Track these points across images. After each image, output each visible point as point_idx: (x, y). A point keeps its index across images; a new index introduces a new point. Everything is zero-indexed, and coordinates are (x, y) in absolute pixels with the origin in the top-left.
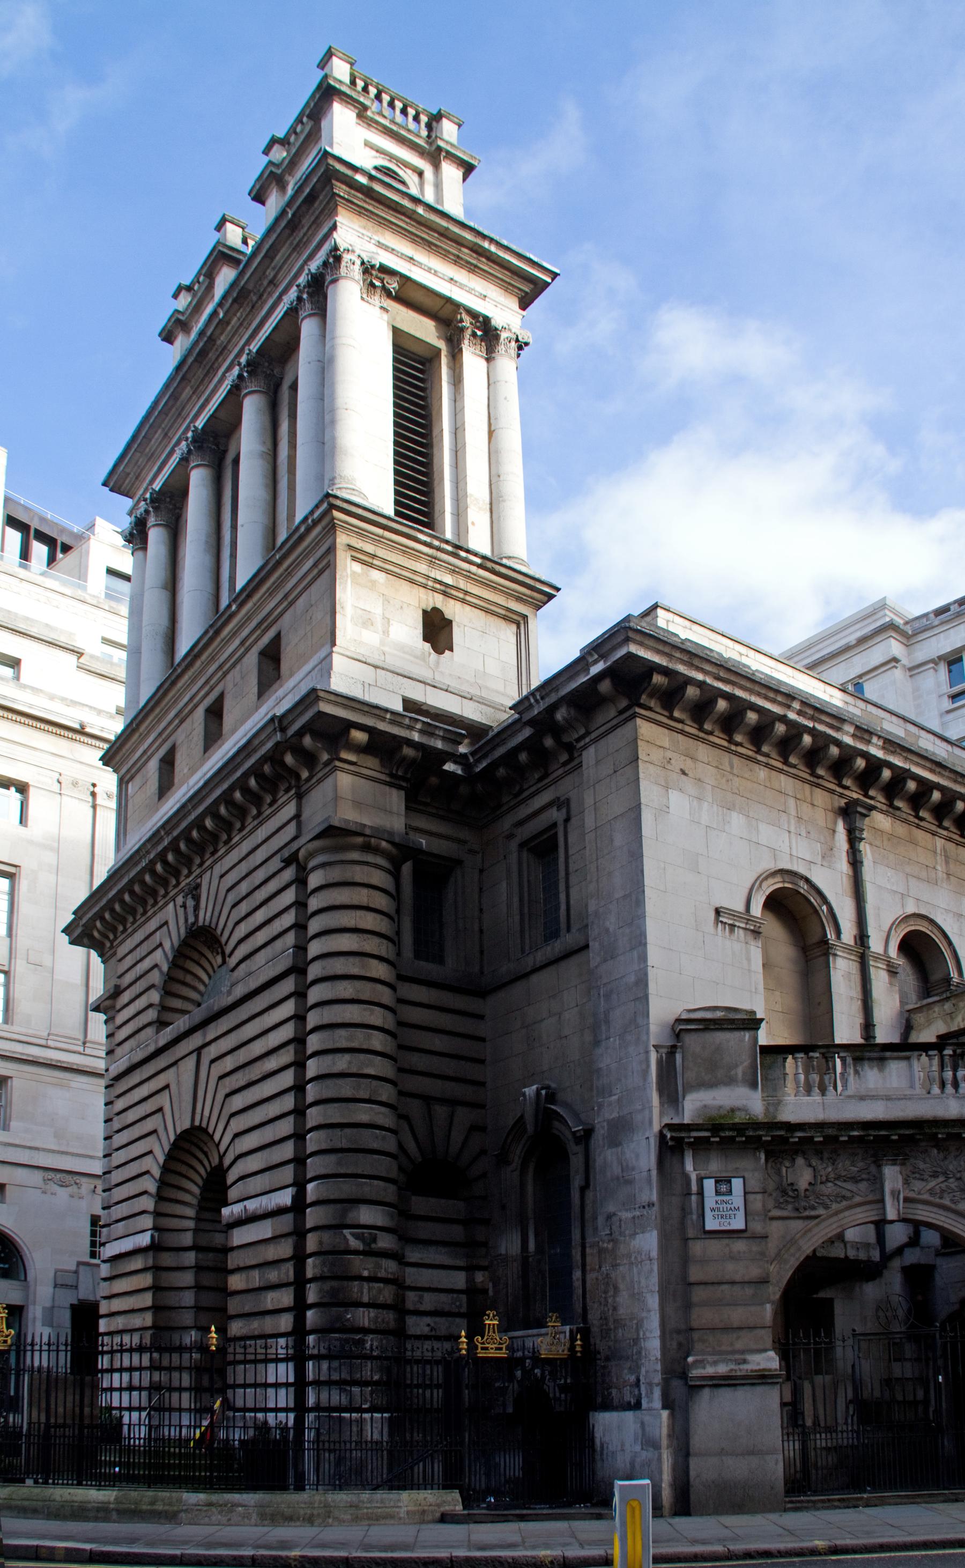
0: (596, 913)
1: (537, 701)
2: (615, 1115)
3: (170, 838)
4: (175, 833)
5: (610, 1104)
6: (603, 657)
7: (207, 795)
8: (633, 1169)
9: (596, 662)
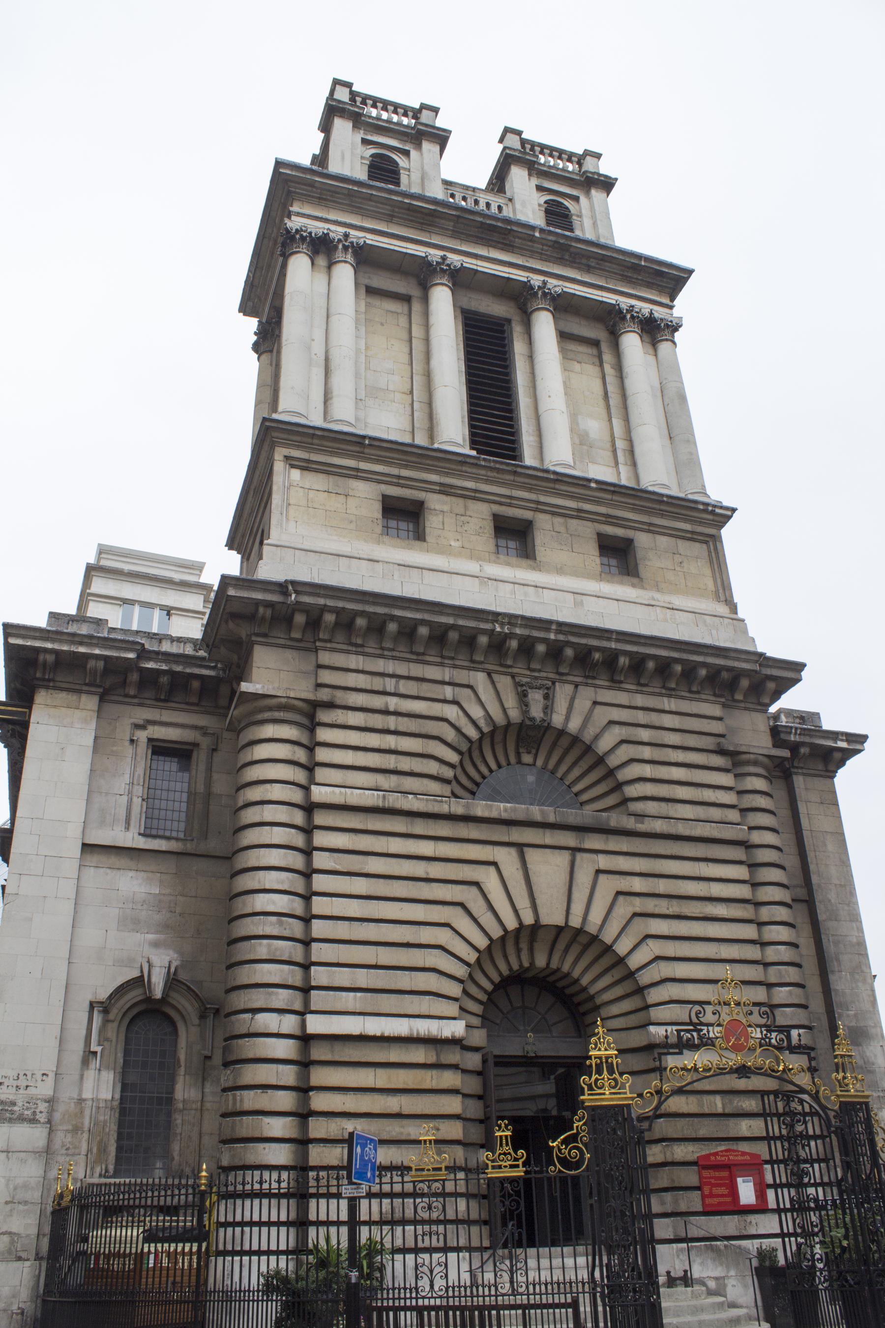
0: (819, 885)
1: (796, 733)
2: (853, 1024)
4: (572, 639)
5: (848, 1016)
6: (848, 741)
7: (645, 645)
8: (873, 1064)
9: (842, 740)
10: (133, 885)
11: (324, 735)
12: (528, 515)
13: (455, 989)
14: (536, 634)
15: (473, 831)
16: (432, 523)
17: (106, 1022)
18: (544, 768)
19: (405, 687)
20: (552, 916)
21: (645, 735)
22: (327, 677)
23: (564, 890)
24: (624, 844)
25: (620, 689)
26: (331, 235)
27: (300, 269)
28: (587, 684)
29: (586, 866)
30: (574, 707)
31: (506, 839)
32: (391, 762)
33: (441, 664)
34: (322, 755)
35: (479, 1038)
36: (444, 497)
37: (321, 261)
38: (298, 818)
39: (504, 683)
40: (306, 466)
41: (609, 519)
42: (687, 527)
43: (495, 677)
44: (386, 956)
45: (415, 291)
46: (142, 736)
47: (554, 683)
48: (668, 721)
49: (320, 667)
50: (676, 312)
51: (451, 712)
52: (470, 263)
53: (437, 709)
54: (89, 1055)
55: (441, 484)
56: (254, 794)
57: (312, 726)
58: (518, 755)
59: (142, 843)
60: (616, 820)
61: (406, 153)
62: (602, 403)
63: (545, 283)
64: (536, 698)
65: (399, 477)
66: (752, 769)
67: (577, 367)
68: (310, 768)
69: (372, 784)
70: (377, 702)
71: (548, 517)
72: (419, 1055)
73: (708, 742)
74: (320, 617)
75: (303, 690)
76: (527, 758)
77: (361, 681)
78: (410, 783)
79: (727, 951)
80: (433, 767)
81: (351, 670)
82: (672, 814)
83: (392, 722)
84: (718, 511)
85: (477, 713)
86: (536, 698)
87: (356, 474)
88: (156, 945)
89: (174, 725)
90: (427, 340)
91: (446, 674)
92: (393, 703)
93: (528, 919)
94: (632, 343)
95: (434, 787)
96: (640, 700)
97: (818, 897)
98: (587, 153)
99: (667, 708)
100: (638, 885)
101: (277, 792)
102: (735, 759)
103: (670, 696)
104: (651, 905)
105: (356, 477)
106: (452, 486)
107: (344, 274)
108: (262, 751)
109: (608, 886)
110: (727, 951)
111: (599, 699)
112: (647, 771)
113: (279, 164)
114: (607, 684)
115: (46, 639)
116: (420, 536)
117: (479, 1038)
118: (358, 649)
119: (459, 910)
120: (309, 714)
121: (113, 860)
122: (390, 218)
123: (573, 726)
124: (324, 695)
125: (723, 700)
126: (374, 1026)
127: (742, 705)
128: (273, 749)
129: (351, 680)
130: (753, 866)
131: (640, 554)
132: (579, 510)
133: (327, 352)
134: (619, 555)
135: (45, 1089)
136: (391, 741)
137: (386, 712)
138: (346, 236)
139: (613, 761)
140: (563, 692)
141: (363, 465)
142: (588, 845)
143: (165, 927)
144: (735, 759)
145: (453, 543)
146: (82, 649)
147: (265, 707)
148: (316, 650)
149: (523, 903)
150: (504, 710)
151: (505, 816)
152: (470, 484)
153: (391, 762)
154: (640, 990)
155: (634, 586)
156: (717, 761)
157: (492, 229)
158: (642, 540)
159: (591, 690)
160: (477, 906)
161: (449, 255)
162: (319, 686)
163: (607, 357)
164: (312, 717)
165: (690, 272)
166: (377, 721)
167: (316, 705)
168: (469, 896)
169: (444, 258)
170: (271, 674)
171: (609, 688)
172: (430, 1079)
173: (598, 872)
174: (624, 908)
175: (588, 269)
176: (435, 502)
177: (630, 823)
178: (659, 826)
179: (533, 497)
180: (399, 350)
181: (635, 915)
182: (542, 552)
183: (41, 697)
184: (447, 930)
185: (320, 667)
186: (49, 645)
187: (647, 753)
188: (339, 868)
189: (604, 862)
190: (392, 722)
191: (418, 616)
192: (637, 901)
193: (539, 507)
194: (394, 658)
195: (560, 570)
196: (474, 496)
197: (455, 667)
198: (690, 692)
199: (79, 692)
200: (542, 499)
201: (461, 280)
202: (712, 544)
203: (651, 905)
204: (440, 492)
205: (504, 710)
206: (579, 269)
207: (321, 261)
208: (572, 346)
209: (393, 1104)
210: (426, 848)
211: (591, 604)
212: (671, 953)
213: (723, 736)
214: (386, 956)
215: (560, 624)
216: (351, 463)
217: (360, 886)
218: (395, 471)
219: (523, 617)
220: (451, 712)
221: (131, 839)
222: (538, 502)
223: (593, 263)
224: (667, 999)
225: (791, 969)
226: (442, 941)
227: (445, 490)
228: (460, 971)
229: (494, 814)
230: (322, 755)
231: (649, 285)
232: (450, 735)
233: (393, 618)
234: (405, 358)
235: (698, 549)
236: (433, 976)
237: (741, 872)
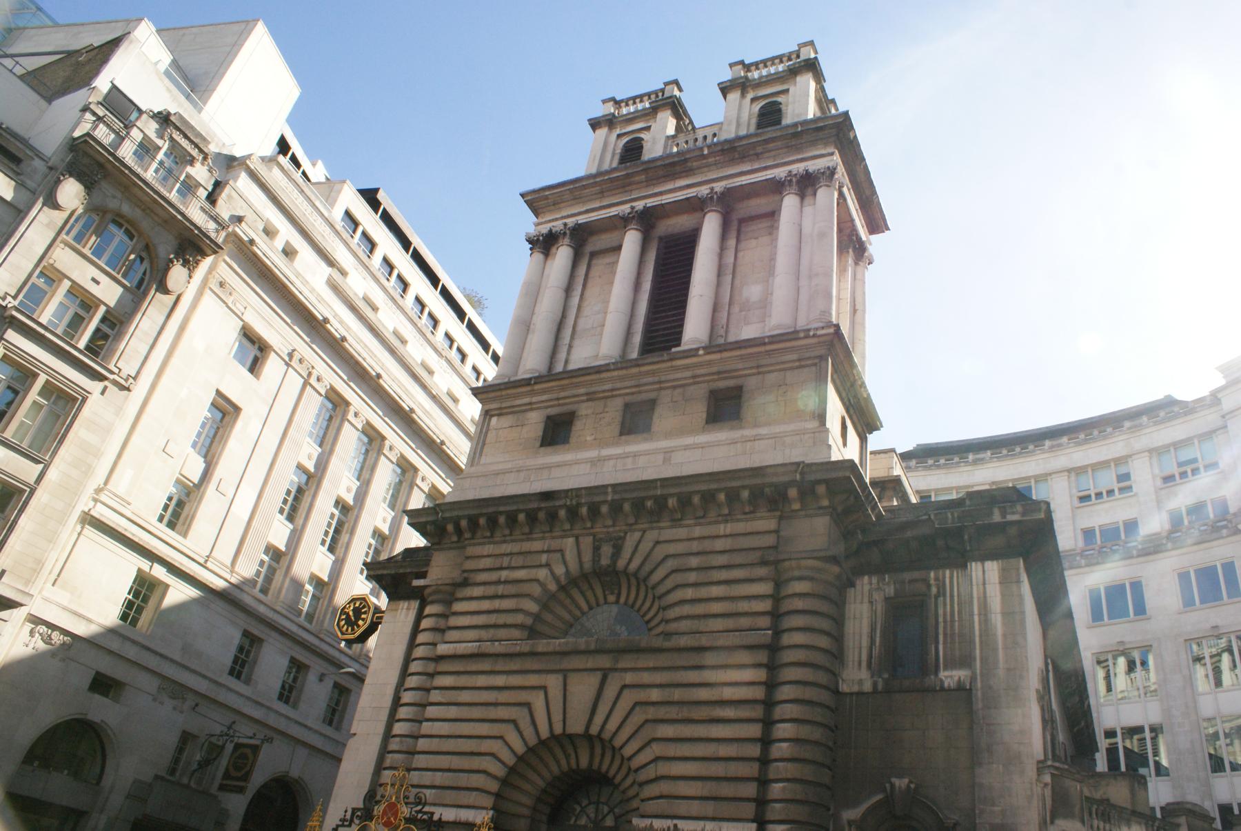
3: (616, 497)
11: (458, 607)
12: (652, 395)
14: (597, 499)
18: (626, 603)
21: (694, 562)
22: (470, 565)
23: (590, 705)
24: (650, 661)
25: (681, 526)
28: (652, 529)
31: (558, 667)
32: (492, 619)
33: (543, 538)
36: (590, 403)
42: (795, 357)
43: (581, 539)
44: (456, 762)
47: (626, 533)
48: (719, 545)
49: (468, 558)
51: (542, 574)
52: (650, 202)
53: (532, 573)
55: (587, 394)
58: (605, 598)
61: (648, 128)
63: (712, 189)
64: (607, 550)
65: (558, 399)
67: (753, 243)
69: (477, 638)
70: (494, 576)
71: (669, 392)
74: (516, 516)
76: (612, 598)
77: (486, 563)
78: (502, 633)
79: (724, 751)
82: (702, 628)
83: (500, 589)
84: (819, 332)
86: (607, 550)
87: (530, 407)
92: (504, 574)
93: (558, 730)
94: (790, 202)
95: (516, 633)
96: (698, 531)
99: (722, 533)
100: (655, 695)
103: (726, 521)
104: (662, 712)
105: (532, 409)
106: (594, 393)
109: (628, 698)
111: (661, 539)
112: (689, 593)
114: (668, 524)
115: (384, 568)
118: (491, 539)
119: (511, 726)
122: (602, 194)
124: (459, 580)
125: (778, 513)
127: (803, 513)
132: (694, 377)
137: (498, 582)
138: (565, 225)
142: (620, 666)
145: (588, 438)
146: (401, 571)
148: (464, 547)
150: (581, 562)
151: (558, 649)
153: (492, 619)
155: (732, 428)
156: (762, 571)
157: (673, 164)
158: (751, 383)
159: (656, 532)
160: (525, 724)
161: (634, 204)
162: (464, 571)
164: (453, 594)
166: (490, 590)
169: (633, 208)
171: (672, 527)
173: (625, 687)
175: (758, 156)
176: (584, 409)
177: (658, 642)
178: (683, 641)
179: (656, 379)
181: (647, 721)
184: (500, 742)
185: (468, 558)
186: (385, 572)
188: (443, 700)
189: (629, 678)
190: (500, 589)
191: (515, 508)
192: (651, 710)
194: (513, 541)
195: (668, 435)
197: (553, 538)
198: (745, 513)
200: (663, 378)
201: (646, 220)
203: (662, 712)
204: (588, 400)
205: (581, 562)
206: (750, 161)
210: (500, 681)
212: (671, 753)
213: (775, 548)
214: (456, 762)
215: (614, 486)
217: (453, 712)
218: (555, 396)
219: (586, 488)
220: (542, 574)
222: (660, 382)
223: (759, 150)
224: (658, 794)
225: (789, 765)
226: (494, 750)
227: (591, 397)
229: (550, 649)
230: (453, 621)
232: (536, 590)
233: (501, 513)
236: (482, 777)
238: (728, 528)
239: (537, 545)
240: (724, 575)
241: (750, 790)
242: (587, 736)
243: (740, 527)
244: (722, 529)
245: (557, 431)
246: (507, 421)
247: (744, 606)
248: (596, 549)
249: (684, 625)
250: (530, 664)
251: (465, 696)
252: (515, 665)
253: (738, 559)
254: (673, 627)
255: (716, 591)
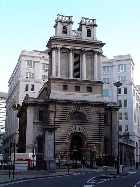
10: (38, 126)
12: (79, 85)
13: (68, 138)
15: (70, 123)
16: (68, 88)
17: (36, 139)
19: (65, 108)
20: (78, 131)
21: (89, 112)
22: (57, 108)
26: (57, 47)
27: (54, 53)
29: (81, 126)
30: (82, 109)
34: (56, 116)
35: (70, 142)
37: (56, 50)
38: (54, 123)
39: (75, 107)
40: (54, 82)
41: (89, 85)
44: (62, 135)
45: (68, 52)
46: (38, 110)
48: (92, 110)
50: (103, 50)
51: (69, 111)
54: (35, 143)
56: (50, 120)
57: (55, 113)
59: (39, 122)
60: (85, 122)
62: (91, 65)
66: (102, 115)
67: (89, 60)
68: (55, 117)
72: (64, 144)
73: (96, 112)
75: (54, 110)
79: (95, 134)
80: (67, 117)
81: (59, 107)
83: (63, 112)
85: (72, 111)
87: (60, 83)
88: (41, 132)
89: (41, 109)
90: (69, 62)
91: (69, 107)
92: (63, 110)
95: (67, 119)
96: (89, 108)
97: (112, 126)
98: (94, 19)
100: (87, 128)
101: (52, 120)
102: (100, 114)
104: (88, 130)
107: (59, 53)
108: (51, 116)
110: (95, 134)
113: (51, 38)
116: (67, 89)
117: (70, 142)
120: (55, 112)
121: (36, 124)
123: (82, 111)
126: (60, 141)
128: (52, 116)
129: (59, 108)
130: (100, 125)
131: (92, 88)
133: (57, 65)
134: (90, 89)
135: (32, 146)
136: (63, 114)
139: (85, 115)
140: (81, 108)
141: (61, 82)
143: (41, 130)
144: (100, 114)
147: (51, 112)
149: (75, 130)
152: (73, 82)
154: (86, 138)
158: (93, 87)
160: (71, 131)
163: (93, 58)
165: (105, 44)
166: (62, 112)
167: (55, 111)
168: (70, 129)
170: (51, 108)
172: (65, 146)
174: (85, 130)
176: (69, 85)
177: (86, 122)
178: (90, 122)
180: (66, 61)
182: (80, 90)
183: (28, 107)
187: (89, 114)
189: (83, 126)
190: (63, 112)
193: (80, 84)
196: (74, 84)
199: (32, 106)
202: (102, 86)
203: (88, 130)
207: (56, 50)
208: (89, 56)
209: (62, 148)
210: (66, 125)
211: (86, 97)
214: (62, 135)
216: (59, 81)
220: (69, 111)
221: (38, 121)
227: (70, 83)
228: (68, 136)
230: (56, 116)
231: (99, 46)
232: (69, 113)
234: (66, 62)
235: (100, 87)
237: (98, 126)
238: (93, 108)
239: (67, 107)
240: (93, 114)
241: (98, 139)
242: (79, 133)
243: (94, 108)
244: (92, 108)
245: (65, 88)
246: (56, 84)
247: (96, 118)
248: (76, 108)
249: (89, 120)
250: (69, 123)
251: (61, 127)
252: (68, 123)
253: (95, 112)
254: (87, 120)
255: (93, 116)
